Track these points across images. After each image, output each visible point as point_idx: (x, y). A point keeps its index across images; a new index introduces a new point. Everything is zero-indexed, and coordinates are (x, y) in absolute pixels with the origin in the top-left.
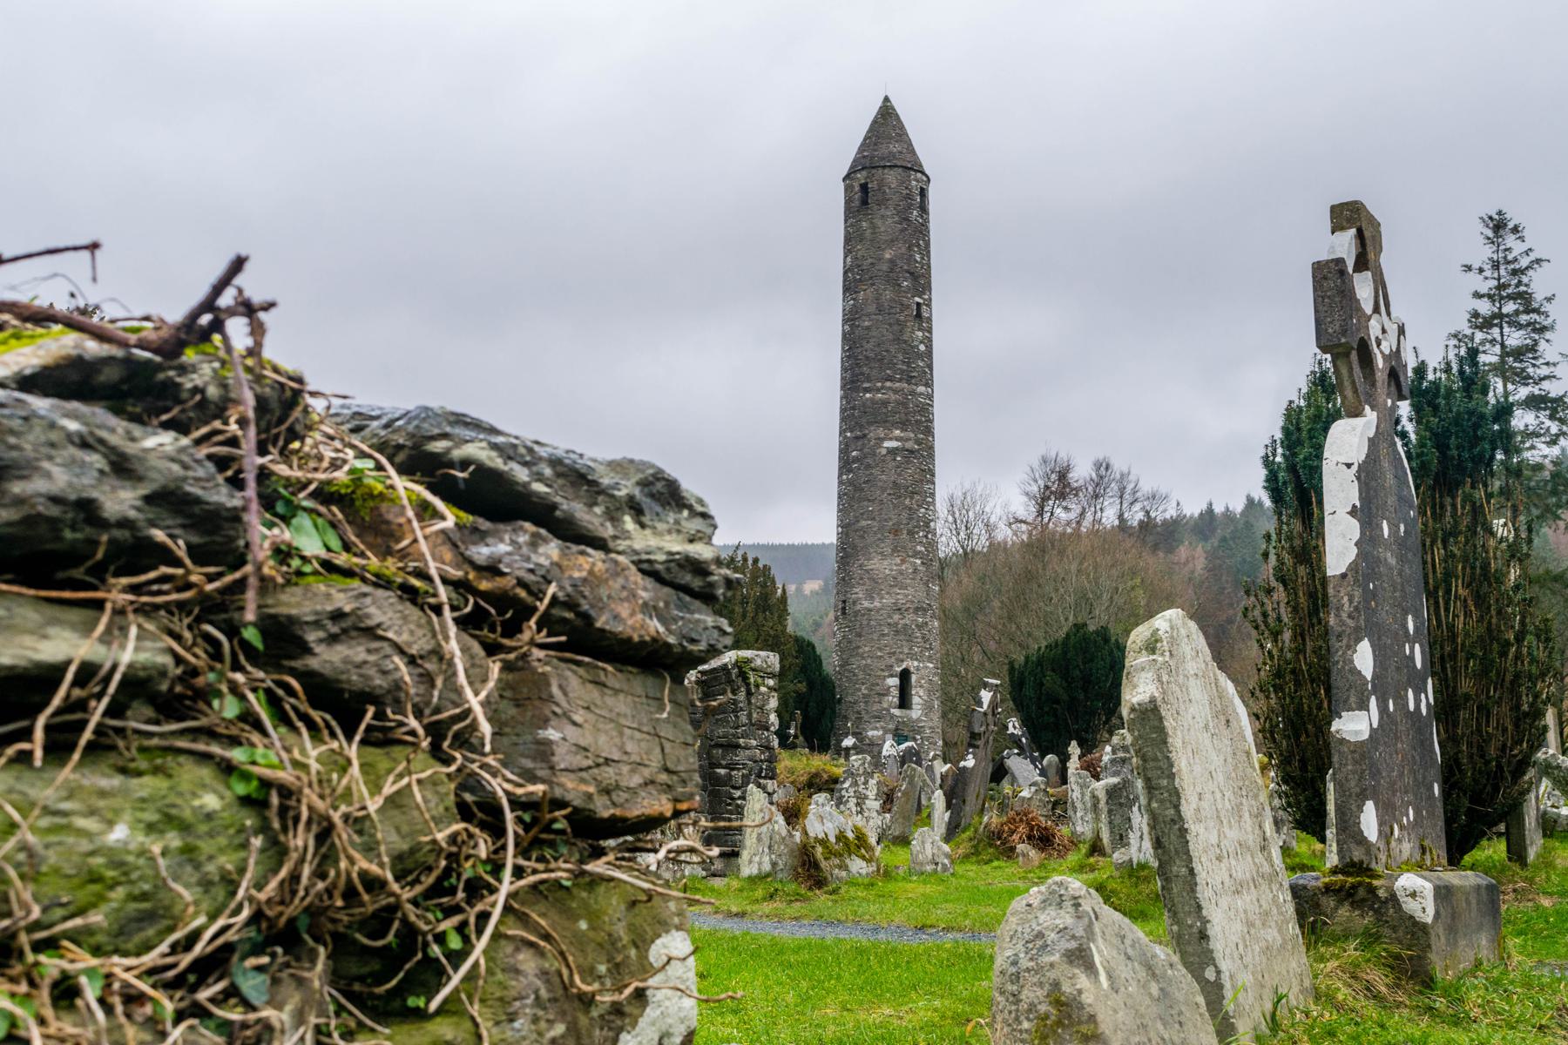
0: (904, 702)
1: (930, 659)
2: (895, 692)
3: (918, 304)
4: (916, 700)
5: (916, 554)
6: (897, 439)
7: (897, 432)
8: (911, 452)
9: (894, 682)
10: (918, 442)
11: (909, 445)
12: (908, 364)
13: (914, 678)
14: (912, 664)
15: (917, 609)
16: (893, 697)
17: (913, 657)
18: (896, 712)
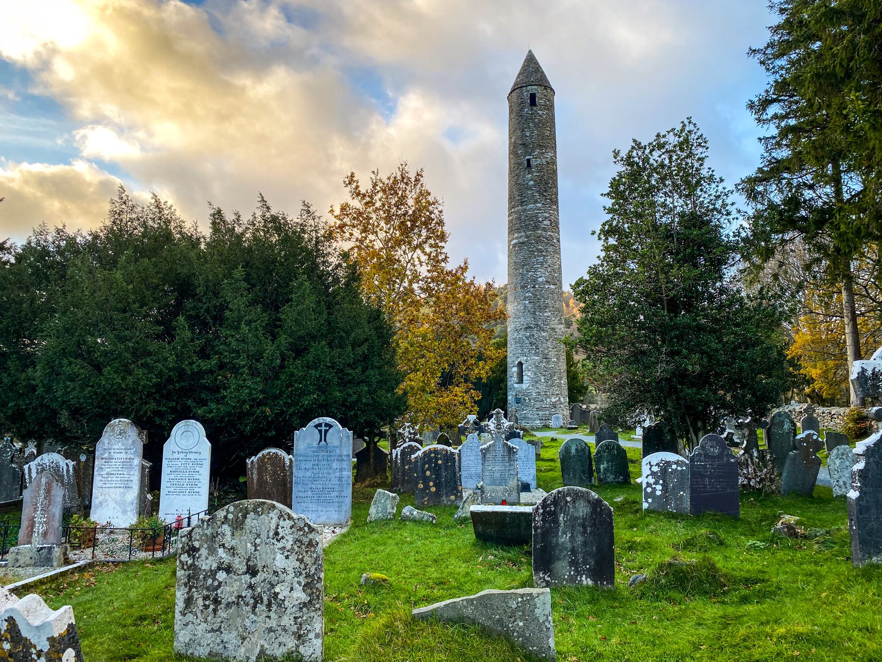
0: (521, 381)
1: (536, 354)
2: (515, 375)
3: (528, 160)
4: (525, 378)
5: (525, 299)
6: (516, 238)
7: (516, 235)
8: (523, 243)
9: (515, 369)
10: (527, 237)
11: (521, 240)
12: (521, 195)
13: (524, 366)
14: (523, 359)
15: (526, 328)
16: (515, 379)
17: (524, 354)
18: (516, 386)
